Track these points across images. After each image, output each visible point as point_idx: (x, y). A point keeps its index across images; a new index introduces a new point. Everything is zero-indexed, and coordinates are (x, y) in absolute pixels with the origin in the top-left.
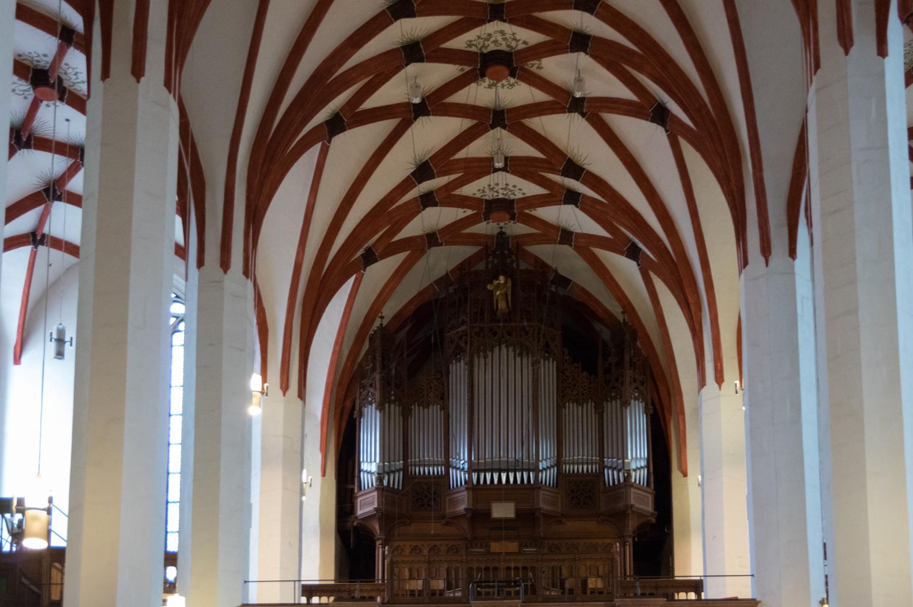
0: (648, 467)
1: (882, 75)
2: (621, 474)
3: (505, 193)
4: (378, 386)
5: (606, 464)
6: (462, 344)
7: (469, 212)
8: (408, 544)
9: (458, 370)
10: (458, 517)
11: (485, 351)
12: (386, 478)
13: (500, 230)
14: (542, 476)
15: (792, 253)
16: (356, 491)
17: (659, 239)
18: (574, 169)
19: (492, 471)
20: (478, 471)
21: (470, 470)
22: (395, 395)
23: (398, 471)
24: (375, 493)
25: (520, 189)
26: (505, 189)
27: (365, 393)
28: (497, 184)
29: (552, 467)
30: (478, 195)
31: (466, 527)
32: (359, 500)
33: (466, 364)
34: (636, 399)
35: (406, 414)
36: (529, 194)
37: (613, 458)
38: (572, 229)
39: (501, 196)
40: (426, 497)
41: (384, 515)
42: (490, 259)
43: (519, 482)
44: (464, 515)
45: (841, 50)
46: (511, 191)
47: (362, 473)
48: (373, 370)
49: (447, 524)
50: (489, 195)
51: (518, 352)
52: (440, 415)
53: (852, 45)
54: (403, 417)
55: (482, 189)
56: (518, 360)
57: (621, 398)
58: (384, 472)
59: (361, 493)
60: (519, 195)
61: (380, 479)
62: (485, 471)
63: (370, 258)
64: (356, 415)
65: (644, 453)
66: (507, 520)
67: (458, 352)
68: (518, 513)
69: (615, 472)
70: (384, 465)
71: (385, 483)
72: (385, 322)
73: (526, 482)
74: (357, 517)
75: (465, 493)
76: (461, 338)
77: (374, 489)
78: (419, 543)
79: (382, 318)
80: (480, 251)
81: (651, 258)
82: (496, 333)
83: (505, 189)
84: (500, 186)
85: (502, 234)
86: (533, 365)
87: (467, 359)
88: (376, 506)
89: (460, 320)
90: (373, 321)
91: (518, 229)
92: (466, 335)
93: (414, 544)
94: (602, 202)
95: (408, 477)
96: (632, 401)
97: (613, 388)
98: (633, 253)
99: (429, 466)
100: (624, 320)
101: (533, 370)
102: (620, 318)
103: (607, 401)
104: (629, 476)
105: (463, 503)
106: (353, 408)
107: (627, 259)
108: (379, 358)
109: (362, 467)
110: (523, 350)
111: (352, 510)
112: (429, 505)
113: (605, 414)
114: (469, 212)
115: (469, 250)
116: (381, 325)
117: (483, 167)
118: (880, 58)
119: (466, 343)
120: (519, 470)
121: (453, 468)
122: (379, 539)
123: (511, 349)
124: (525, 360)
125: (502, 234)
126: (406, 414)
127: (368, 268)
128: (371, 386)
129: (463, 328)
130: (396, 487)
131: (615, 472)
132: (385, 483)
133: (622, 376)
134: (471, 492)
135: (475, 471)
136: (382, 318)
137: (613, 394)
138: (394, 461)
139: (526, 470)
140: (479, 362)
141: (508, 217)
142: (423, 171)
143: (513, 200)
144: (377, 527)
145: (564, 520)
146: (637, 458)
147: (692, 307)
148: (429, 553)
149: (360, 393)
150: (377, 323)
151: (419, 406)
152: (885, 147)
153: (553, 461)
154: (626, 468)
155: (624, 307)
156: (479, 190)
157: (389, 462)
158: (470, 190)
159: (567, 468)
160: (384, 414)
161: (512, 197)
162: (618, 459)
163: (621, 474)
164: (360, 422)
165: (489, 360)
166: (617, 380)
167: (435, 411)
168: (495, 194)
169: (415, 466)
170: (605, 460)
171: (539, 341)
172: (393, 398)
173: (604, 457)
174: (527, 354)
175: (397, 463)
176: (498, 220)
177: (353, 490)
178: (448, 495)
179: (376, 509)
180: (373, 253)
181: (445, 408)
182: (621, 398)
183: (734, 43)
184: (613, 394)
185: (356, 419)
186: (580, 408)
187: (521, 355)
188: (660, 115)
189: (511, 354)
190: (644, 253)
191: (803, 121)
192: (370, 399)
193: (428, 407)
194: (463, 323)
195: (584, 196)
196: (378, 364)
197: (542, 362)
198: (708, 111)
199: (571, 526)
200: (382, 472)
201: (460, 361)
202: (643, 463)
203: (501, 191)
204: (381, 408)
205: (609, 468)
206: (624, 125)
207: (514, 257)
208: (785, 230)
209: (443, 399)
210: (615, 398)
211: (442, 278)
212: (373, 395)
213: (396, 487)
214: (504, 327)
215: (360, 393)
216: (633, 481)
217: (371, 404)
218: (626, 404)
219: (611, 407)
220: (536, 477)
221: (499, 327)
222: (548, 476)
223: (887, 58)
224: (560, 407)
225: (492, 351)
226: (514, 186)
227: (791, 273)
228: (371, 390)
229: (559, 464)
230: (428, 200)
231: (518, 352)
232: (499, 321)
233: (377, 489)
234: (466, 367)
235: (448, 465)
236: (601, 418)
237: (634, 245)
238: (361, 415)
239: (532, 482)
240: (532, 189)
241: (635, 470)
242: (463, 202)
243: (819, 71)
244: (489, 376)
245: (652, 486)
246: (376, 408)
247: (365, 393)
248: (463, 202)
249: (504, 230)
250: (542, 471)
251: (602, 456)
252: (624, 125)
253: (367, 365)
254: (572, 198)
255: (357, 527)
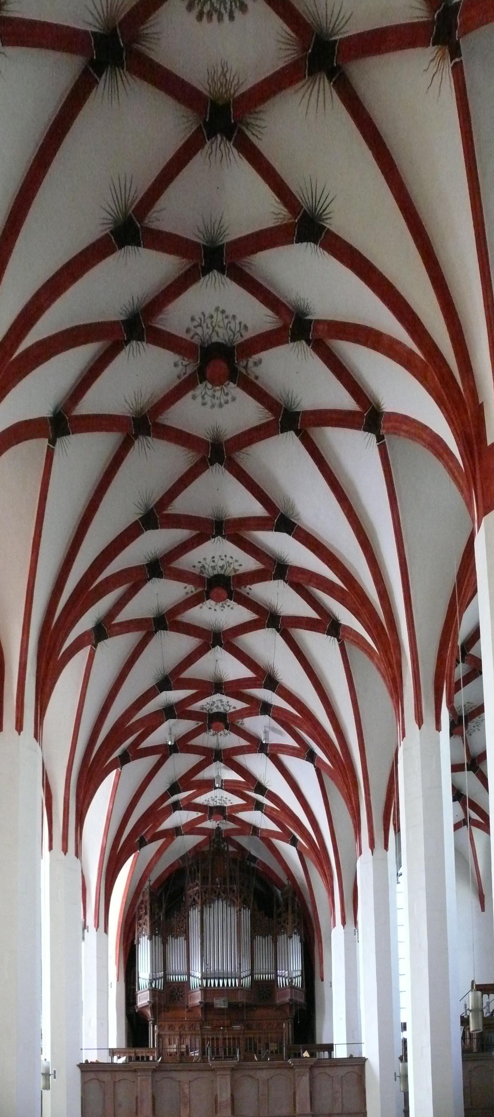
0: (302, 975)
1: (438, 743)
2: (287, 980)
3: (221, 802)
4: (148, 924)
5: (278, 974)
6: (196, 898)
7: (200, 814)
8: (167, 1023)
9: (194, 915)
10: (195, 1007)
11: (210, 903)
12: (154, 982)
13: (217, 826)
14: (243, 981)
15: (386, 847)
16: (137, 990)
17: (310, 835)
18: (261, 789)
19: (214, 978)
20: (207, 979)
21: (202, 978)
22: (159, 930)
23: (161, 978)
24: (148, 992)
25: (229, 800)
26: (221, 800)
27: (140, 929)
28: (216, 797)
29: (249, 976)
30: (205, 803)
31: (200, 1013)
32: (139, 996)
33: (198, 911)
34: (295, 934)
35: (165, 943)
36: (235, 803)
37: (282, 970)
38: (259, 826)
39: (218, 804)
40: (177, 994)
41: (154, 1006)
42: (212, 844)
43: (230, 985)
44: (198, 1006)
45: (417, 726)
46: (224, 801)
47: (140, 979)
48: (146, 914)
49: (189, 1011)
50: (212, 804)
51: (228, 904)
52: (184, 943)
53: (423, 723)
54: (163, 944)
55: (207, 799)
56: (229, 909)
57: (287, 933)
58: (154, 979)
59: (139, 992)
60: (229, 804)
61: (151, 983)
62: (210, 979)
63: (142, 843)
64: (136, 943)
65: (300, 968)
66: (223, 1009)
67: (194, 903)
68: (230, 1005)
69: (284, 979)
70: (153, 975)
71: (154, 986)
72: (152, 883)
73: (233, 985)
74: (137, 1007)
75: (199, 992)
76: (196, 895)
77: (147, 989)
78: (174, 1023)
79: (150, 881)
80: (206, 839)
81: (304, 846)
82: (215, 892)
83: (221, 800)
84: (218, 798)
85: (218, 828)
86: (237, 912)
87: (199, 908)
88: (149, 1000)
89: (195, 883)
90: (145, 882)
91: (227, 825)
92: (199, 893)
93: (170, 1023)
94: (277, 810)
95: (167, 983)
96: (293, 935)
97: (283, 927)
98: (294, 842)
99: (178, 975)
100: (289, 884)
101: (237, 915)
102: (286, 882)
103: (279, 935)
104: (292, 981)
105: (197, 999)
106: (134, 939)
107: (290, 846)
108: (148, 907)
109: (140, 976)
110: (232, 904)
111: (135, 1003)
112: (178, 1000)
113: (278, 943)
114: (200, 814)
115: (200, 838)
116: (150, 885)
117: (208, 785)
118: (437, 732)
119: (199, 898)
120: (229, 978)
121: (192, 976)
122: (150, 1020)
123: (224, 902)
124: (232, 909)
125: (218, 828)
126: (165, 943)
127: (142, 849)
128: (144, 924)
129: (197, 888)
130: (160, 988)
131: (284, 979)
132: (154, 986)
133: (288, 919)
134: (203, 991)
135: (204, 978)
136: (150, 881)
137: (282, 931)
138: (158, 972)
139: (233, 978)
140: (207, 911)
141: (222, 817)
142: (174, 788)
143: (226, 807)
144: (149, 1012)
145: (255, 1008)
146: (296, 970)
147: (328, 877)
148: (179, 1028)
149: (138, 929)
150: (147, 884)
151: (172, 937)
152: (440, 787)
153: (249, 972)
154: (290, 976)
155: (288, 875)
156: (206, 800)
157: (155, 973)
158: (201, 800)
159: (256, 977)
160: (152, 942)
161: (225, 805)
162: (285, 971)
163: (287, 980)
164: (138, 947)
165: (212, 909)
166: (285, 922)
167: (181, 940)
168: (215, 803)
169: (170, 975)
170: (278, 971)
171: (240, 897)
172: (157, 932)
173: (277, 970)
174: (234, 906)
175: (160, 973)
176: (216, 820)
177: (135, 989)
178: (190, 993)
179: (149, 1002)
180: (145, 840)
181: (187, 939)
182: (287, 933)
183: (355, 715)
184: (282, 931)
185: (135, 945)
186: (264, 939)
187: (230, 906)
188: (311, 757)
189: (225, 905)
190: (300, 842)
191: (393, 766)
192: (144, 933)
193: (177, 938)
194: (197, 885)
195: (266, 805)
196: (148, 911)
197: (242, 909)
198: (340, 757)
199: (259, 1012)
200: (151, 978)
201: (195, 909)
202: (299, 973)
203: (218, 801)
204: (150, 938)
205: (280, 976)
206: (290, 762)
207: (225, 844)
208: (382, 833)
209: (186, 933)
210: (284, 933)
211: (184, 855)
212: (146, 930)
213: (160, 988)
214: (220, 887)
215: (138, 929)
216: (294, 984)
217: (145, 936)
218: (291, 937)
219: (282, 939)
220: (240, 982)
221: (217, 888)
222: (247, 982)
223: (441, 732)
224: (253, 938)
225: (214, 903)
226: (226, 798)
227: (385, 860)
228: (144, 927)
229: (252, 975)
230: (176, 806)
231: (228, 904)
232: (217, 884)
233: (149, 989)
234: (199, 913)
235: (189, 975)
236: (276, 946)
237: (294, 837)
238: (138, 943)
239: (237, 985)
240: (237, 801)
241: (295, 978)
242: (196, 808)
243: (404, 738)
244: (212, 919)
245: (304, 988)
246: (148, 939)
247: (140, 929)
248: (196, 808)
249: (219, 826)
250: (243, 979)
251: (276, 969)
252: (290, 762)
253: (142, 911)
254: (259, 806)
255: (137, 1013)
